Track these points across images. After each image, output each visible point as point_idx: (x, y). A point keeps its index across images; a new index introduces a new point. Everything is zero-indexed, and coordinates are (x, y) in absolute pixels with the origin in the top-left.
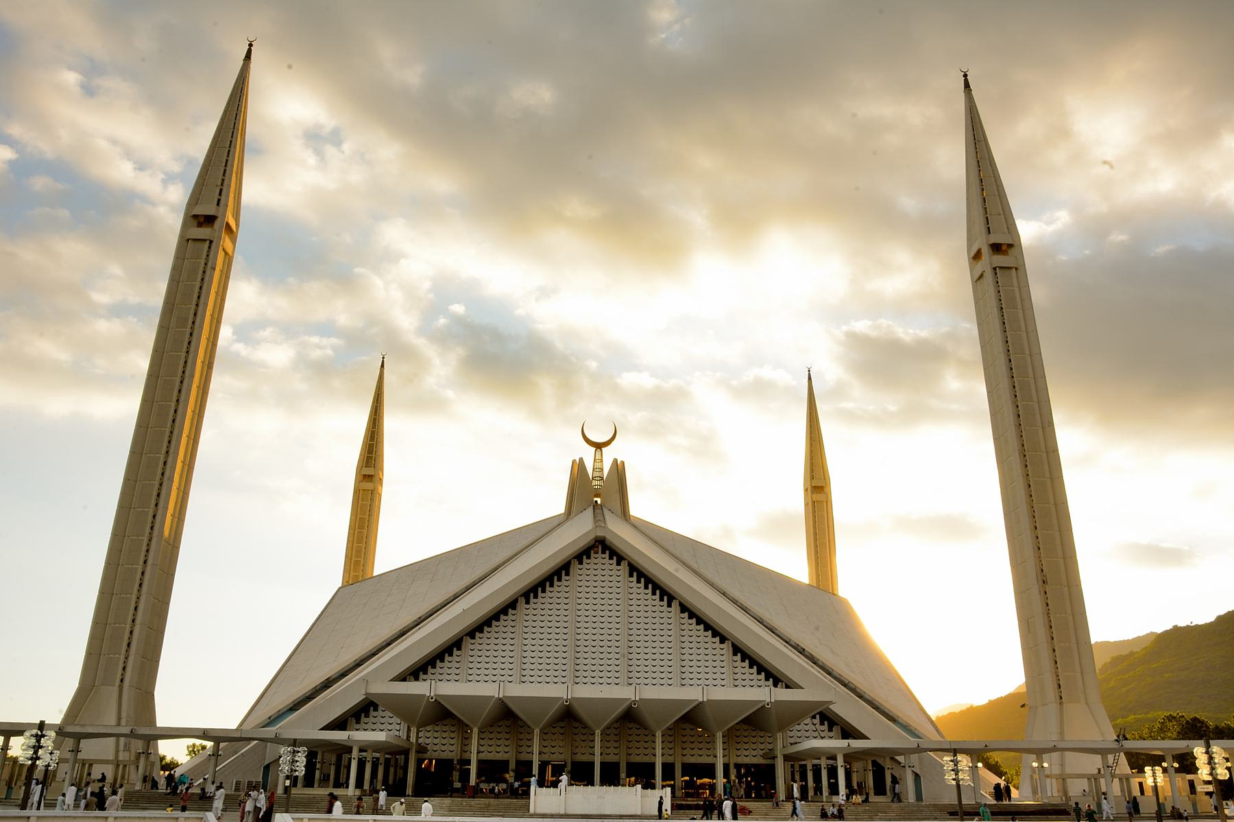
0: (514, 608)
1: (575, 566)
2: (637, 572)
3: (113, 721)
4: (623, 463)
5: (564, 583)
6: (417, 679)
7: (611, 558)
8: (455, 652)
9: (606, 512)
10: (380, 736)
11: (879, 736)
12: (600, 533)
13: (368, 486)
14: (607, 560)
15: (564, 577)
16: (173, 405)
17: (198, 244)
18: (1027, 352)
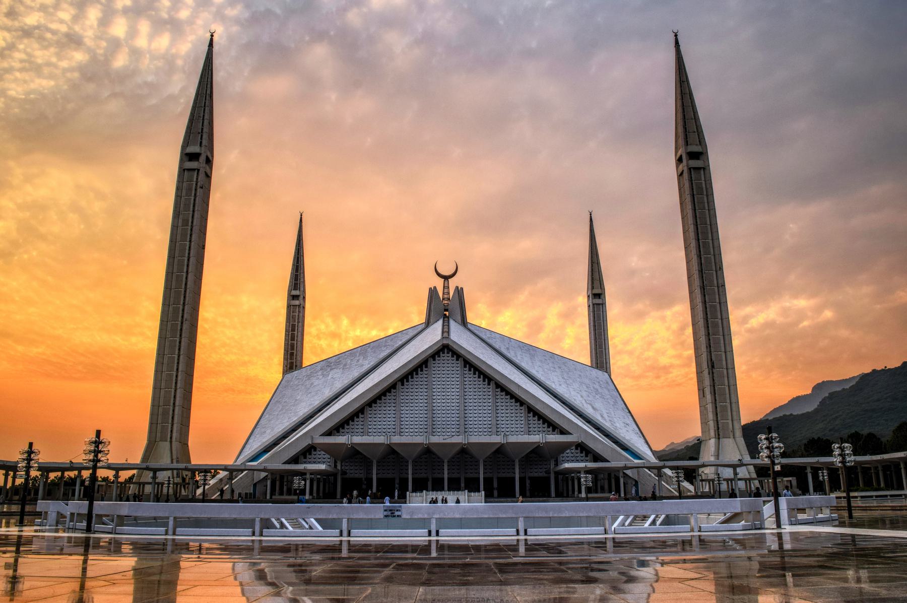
1: (431, 361)
2: (470, 365)
3: (169, 461)
4: (462, 289)
6: (338, 432)
8: (361, 416)
9: (452, 322)
10: (323, 467)
11: (617, 460)
12: (445, 342)
13: (297, 302)
16: (185, 274)
17: (191, 173)
18: (708, 223)
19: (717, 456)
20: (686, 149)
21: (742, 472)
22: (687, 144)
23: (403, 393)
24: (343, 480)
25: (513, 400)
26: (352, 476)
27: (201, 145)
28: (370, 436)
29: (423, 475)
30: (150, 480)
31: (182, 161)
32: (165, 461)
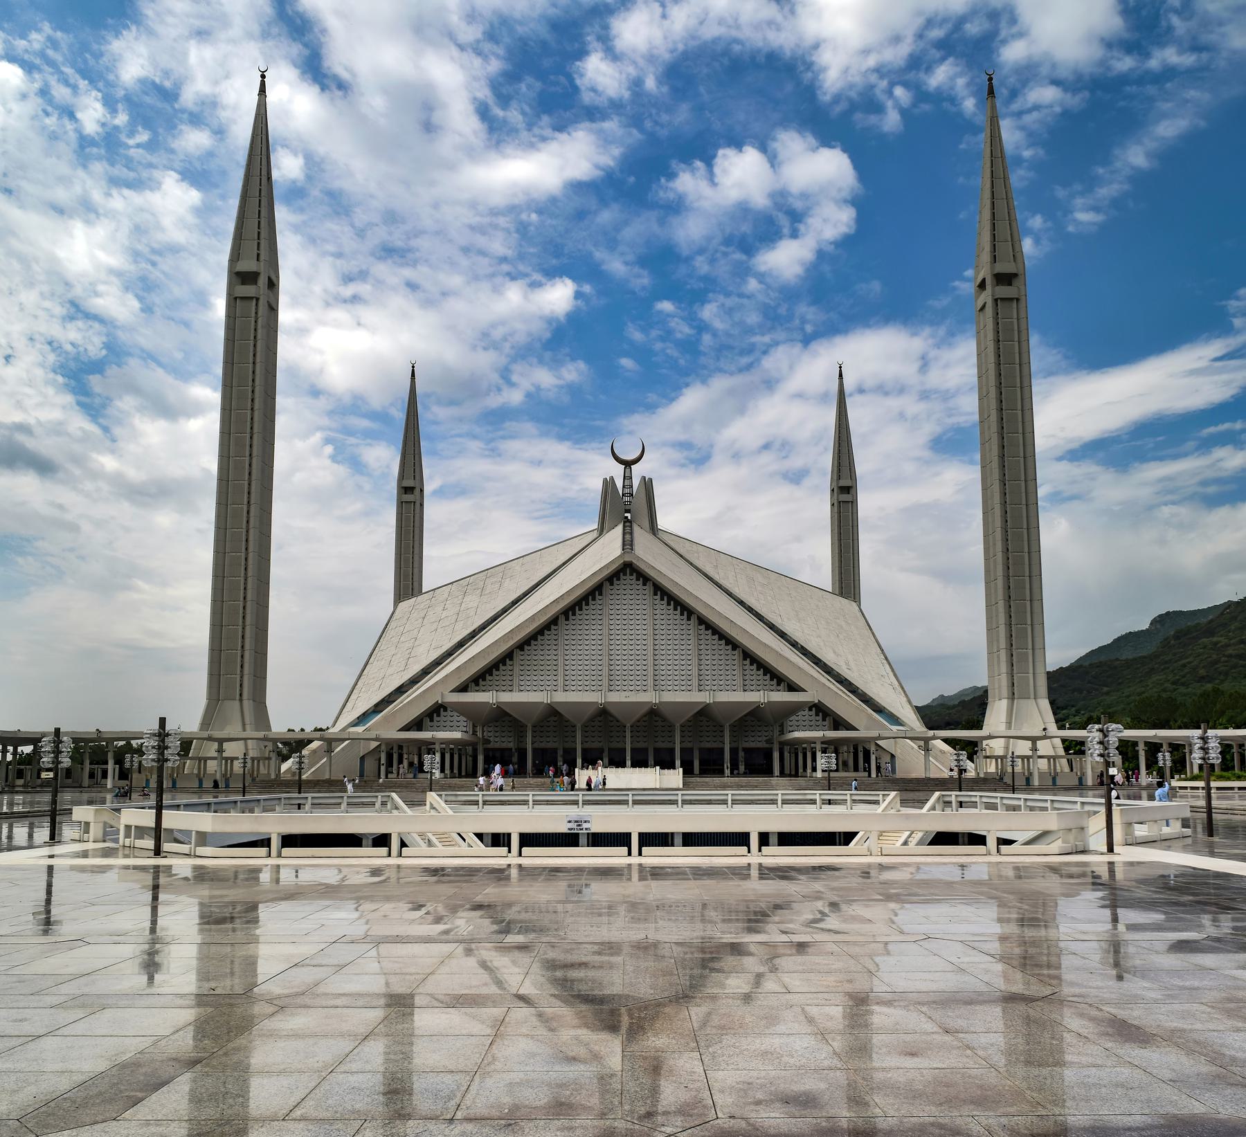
0: (556, 624)
2: (662, 593)
6: (477, 685)
7: (638, 579)
9: (636, 528)
10: (457, 735)
11: (865, 725)
12: (627, 558)
15: (598, 597)
19: (1009, 724)
21: (1044, 747)
23: (565, 631)
24: (486, 750)
25: (723, 642)
26: (497, 746)
28: (523, 694)
30: (215, 755)
32: (234, 729)
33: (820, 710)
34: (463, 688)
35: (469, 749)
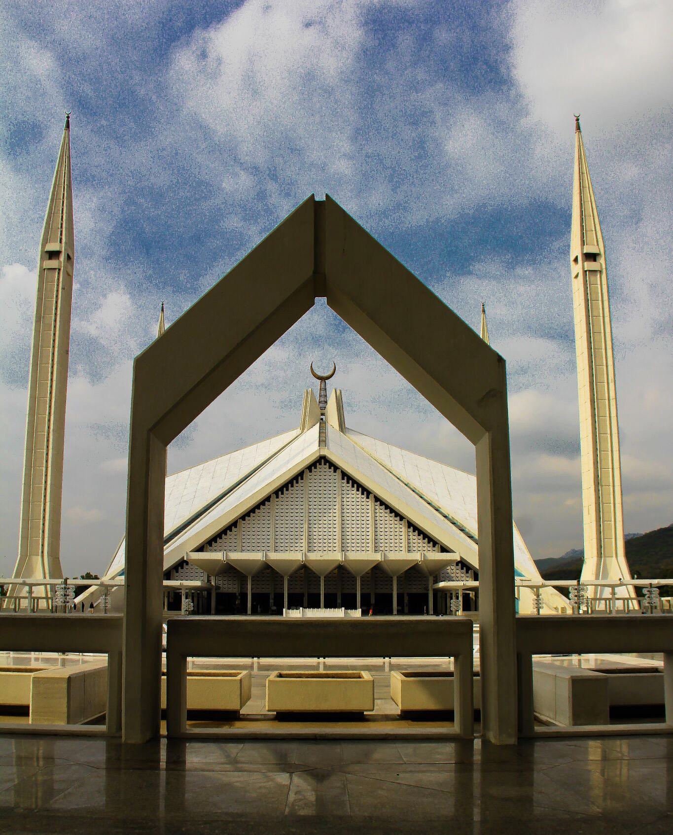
1: (307, 473)
5: (300, 484)
6: (211, 545)
7: (330, 468)
14: (327, 469)
15: (300, 481)
19: (597, 577)
20: (582, 249)
22: (583, 243)
26: (225, 591)
27: (61, 242)
29: (298, 591)
31: (42, 259)
33: (463, 564)
34: (200, 549)
35: (205, 593)
